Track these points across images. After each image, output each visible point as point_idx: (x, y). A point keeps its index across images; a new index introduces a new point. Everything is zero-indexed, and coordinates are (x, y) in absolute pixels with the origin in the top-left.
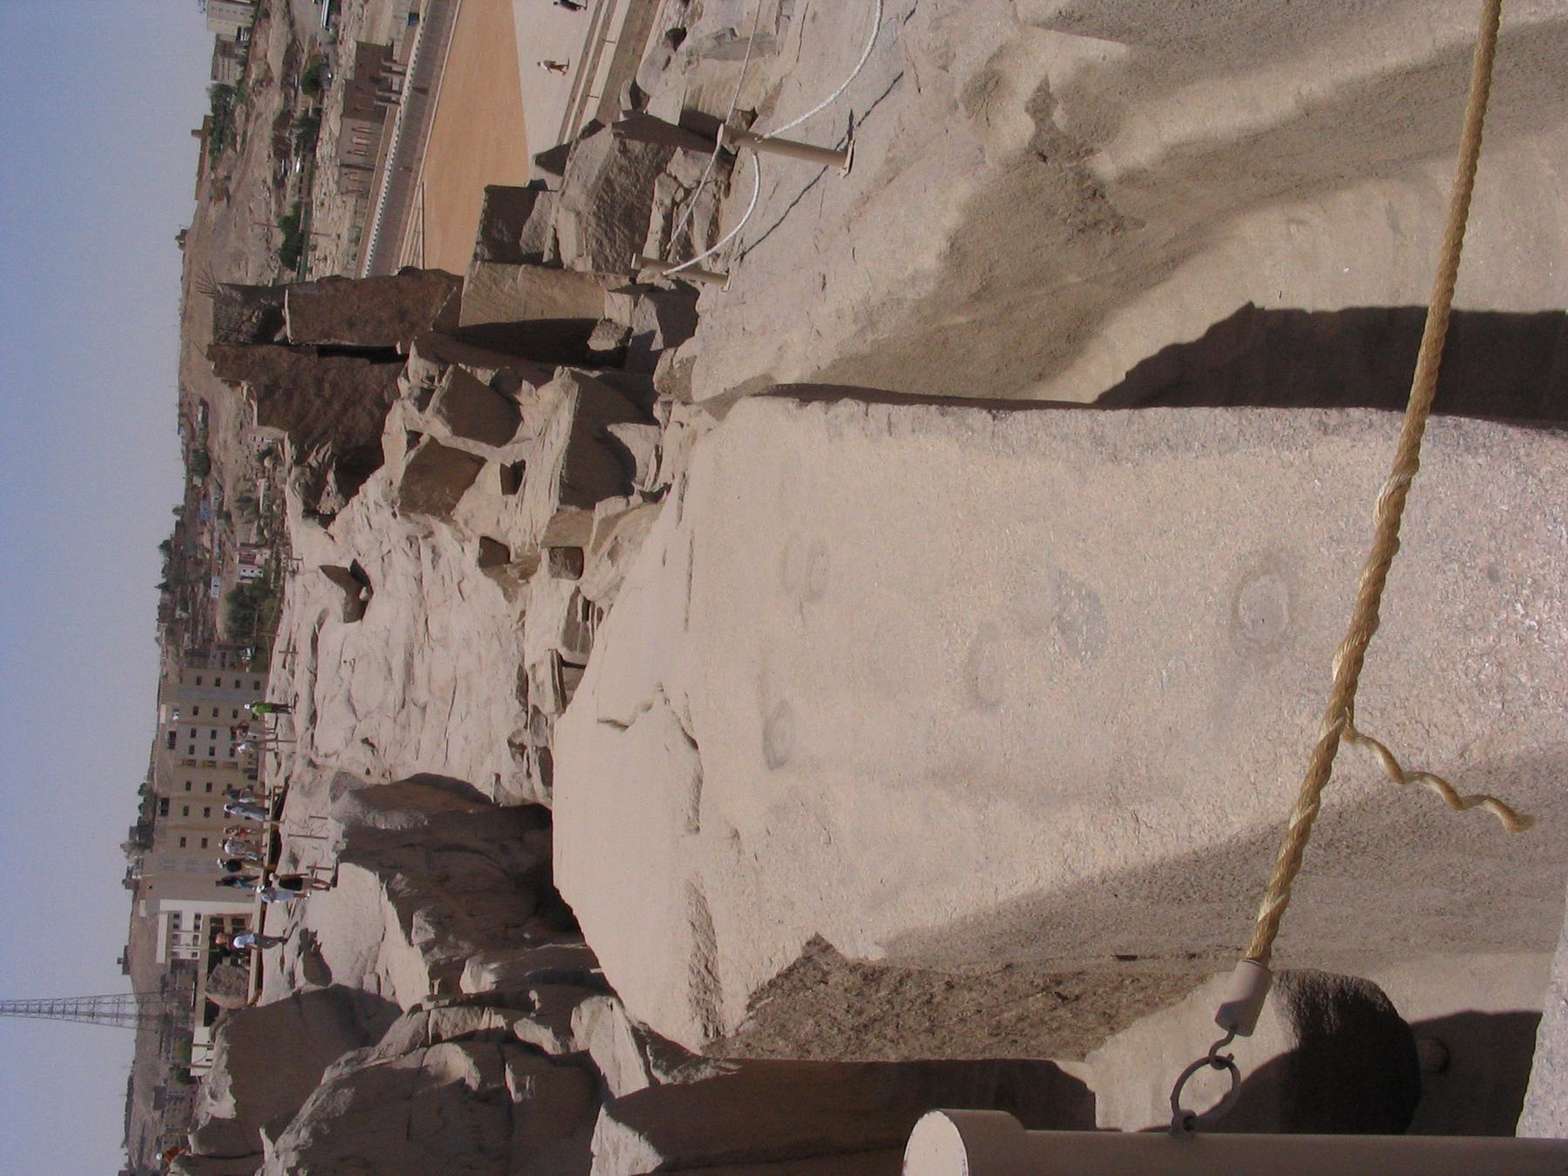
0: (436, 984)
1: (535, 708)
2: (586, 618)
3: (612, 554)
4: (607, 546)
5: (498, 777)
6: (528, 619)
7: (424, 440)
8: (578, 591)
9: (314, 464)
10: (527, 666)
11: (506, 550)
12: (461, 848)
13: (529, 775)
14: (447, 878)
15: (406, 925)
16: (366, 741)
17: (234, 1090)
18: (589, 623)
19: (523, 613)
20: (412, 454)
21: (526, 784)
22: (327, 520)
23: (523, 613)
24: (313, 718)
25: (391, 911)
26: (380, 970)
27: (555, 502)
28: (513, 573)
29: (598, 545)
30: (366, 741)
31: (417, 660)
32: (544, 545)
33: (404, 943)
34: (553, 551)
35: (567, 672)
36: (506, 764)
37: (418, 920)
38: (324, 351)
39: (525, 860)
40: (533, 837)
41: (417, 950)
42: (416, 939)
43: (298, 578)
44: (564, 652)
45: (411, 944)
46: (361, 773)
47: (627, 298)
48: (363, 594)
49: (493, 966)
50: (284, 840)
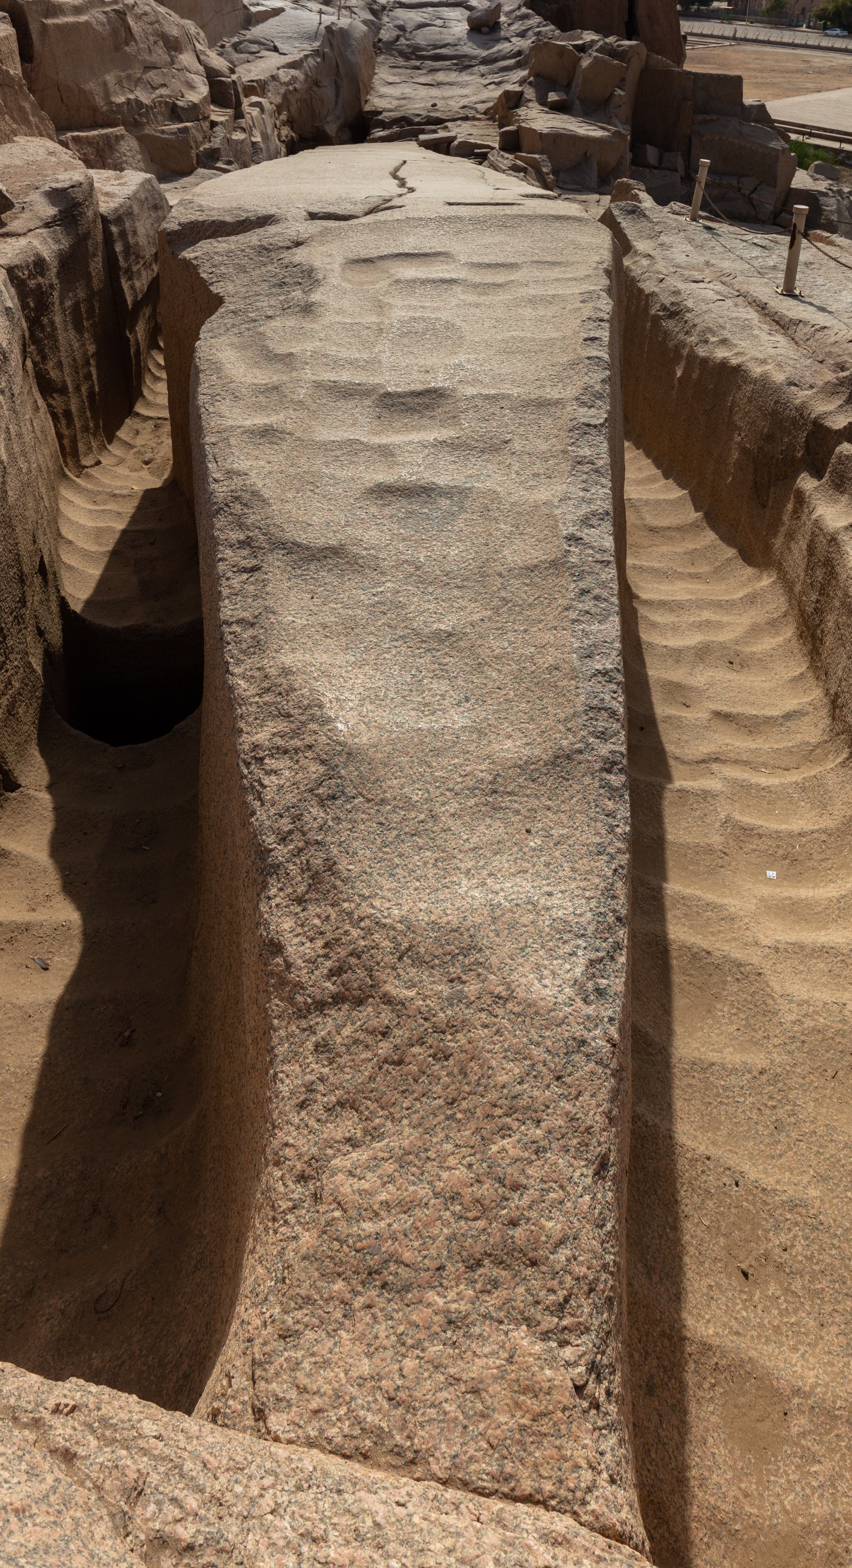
3: (515, 169)
4: (519, 162)
8: (493, 148)
11: (517, 106)
12: (337, 95)
14: (319, 86)
27: (546, 131)
29: (521, 159)
31: (448, 63)
32: (520, 127)
34: (516, 133)
35: (443, 147)
37: (293, 72)
39: (331, 129)
44: (456, 143)
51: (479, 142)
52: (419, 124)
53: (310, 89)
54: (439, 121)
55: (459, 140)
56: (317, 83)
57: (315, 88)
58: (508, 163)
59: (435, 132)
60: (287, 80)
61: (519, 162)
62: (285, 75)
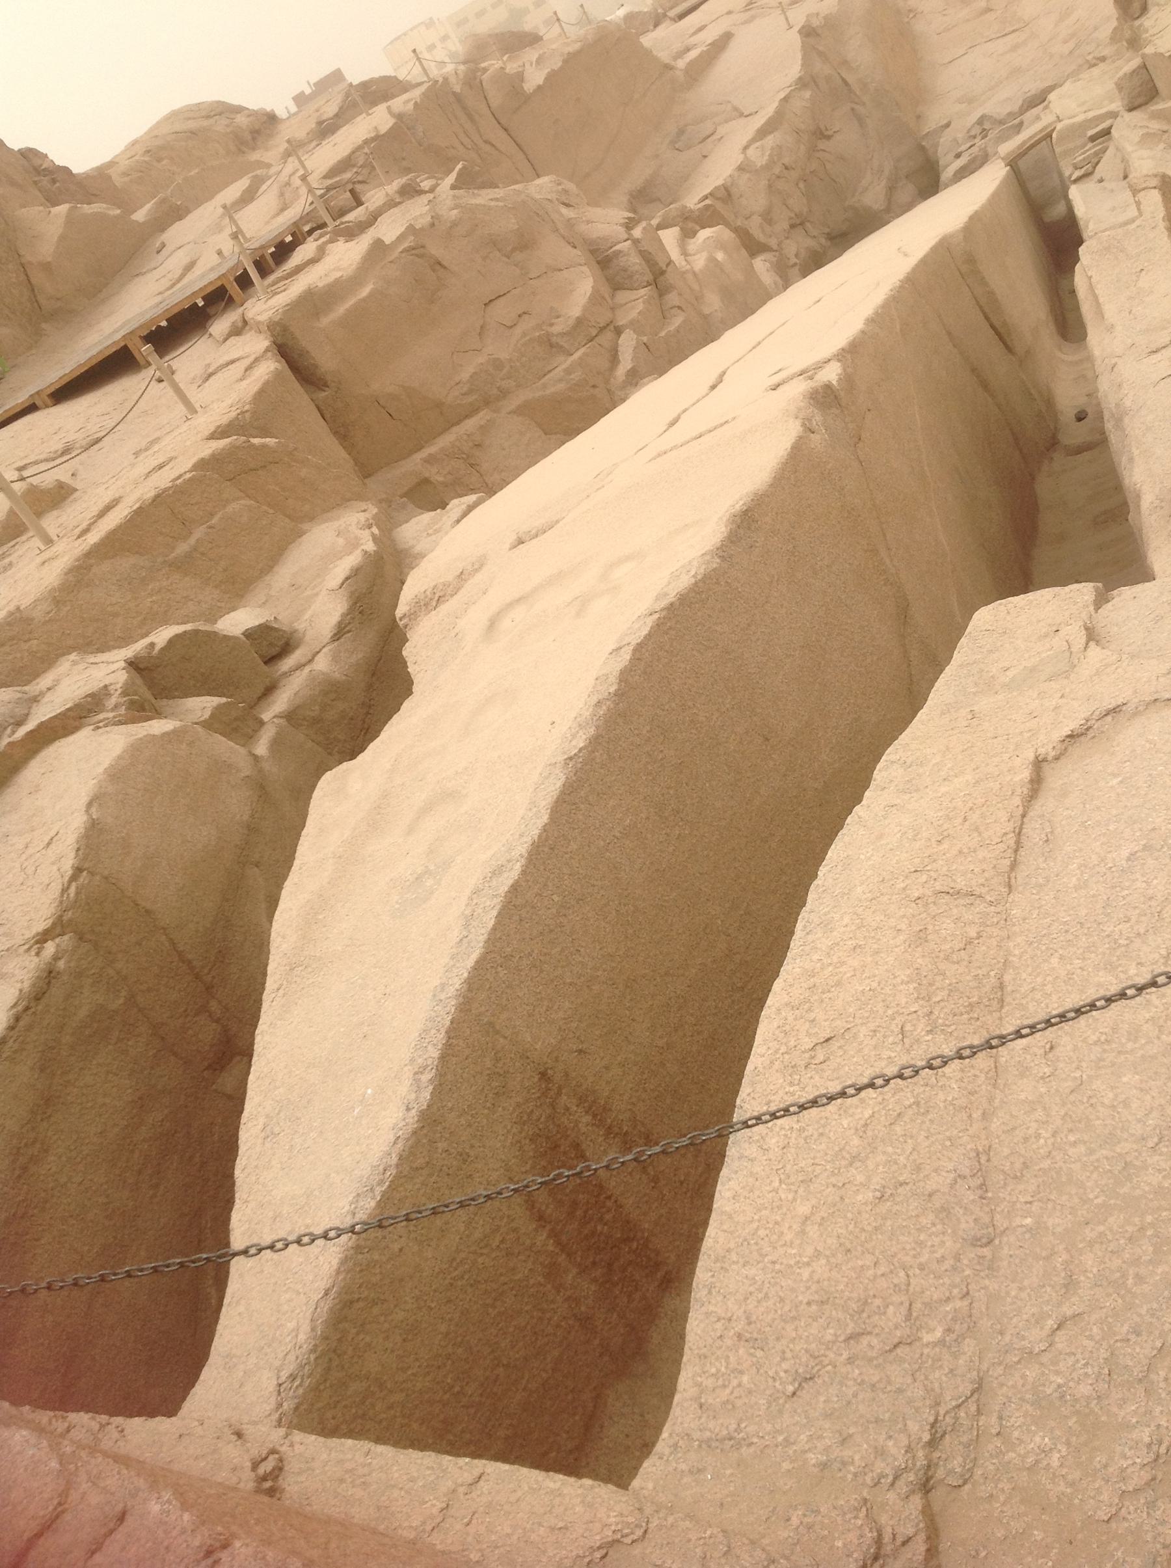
0: (708, 202)
1: (1021, 123)
2: (1093, 139)
5: (948, 125)
8: (1114, 115)
10: (1052, 97)
13: (958, 156)
15: (762, 133)
17: (551, 77)
18: (1090, 145)
19: (1103, 59)
21: (951, 156)
23: (1103, 59)
25: (770, 111)
26: (721, 131)
28: (1128, 34)
32: (1144, 56)
33: (744, 143)
34: (1144, 66)
36: (958, 130)
37: (770, 141)
40: (906, 191)
41: (741, 158)
42: (751, 152)
44: (1054, 135)
45: (746, 148)
49: (720, 256)
51: (1091, 115)
52: (1012, 115)
53: (813, 149)
54: (1039, 99)
55: (1059, 126)
56: (821, 134)
57: (822, 144)
58: (1136, 135)
59: (1038, 118)
60: (764, 160)
61: (1155, 126)
62: (758, 156)
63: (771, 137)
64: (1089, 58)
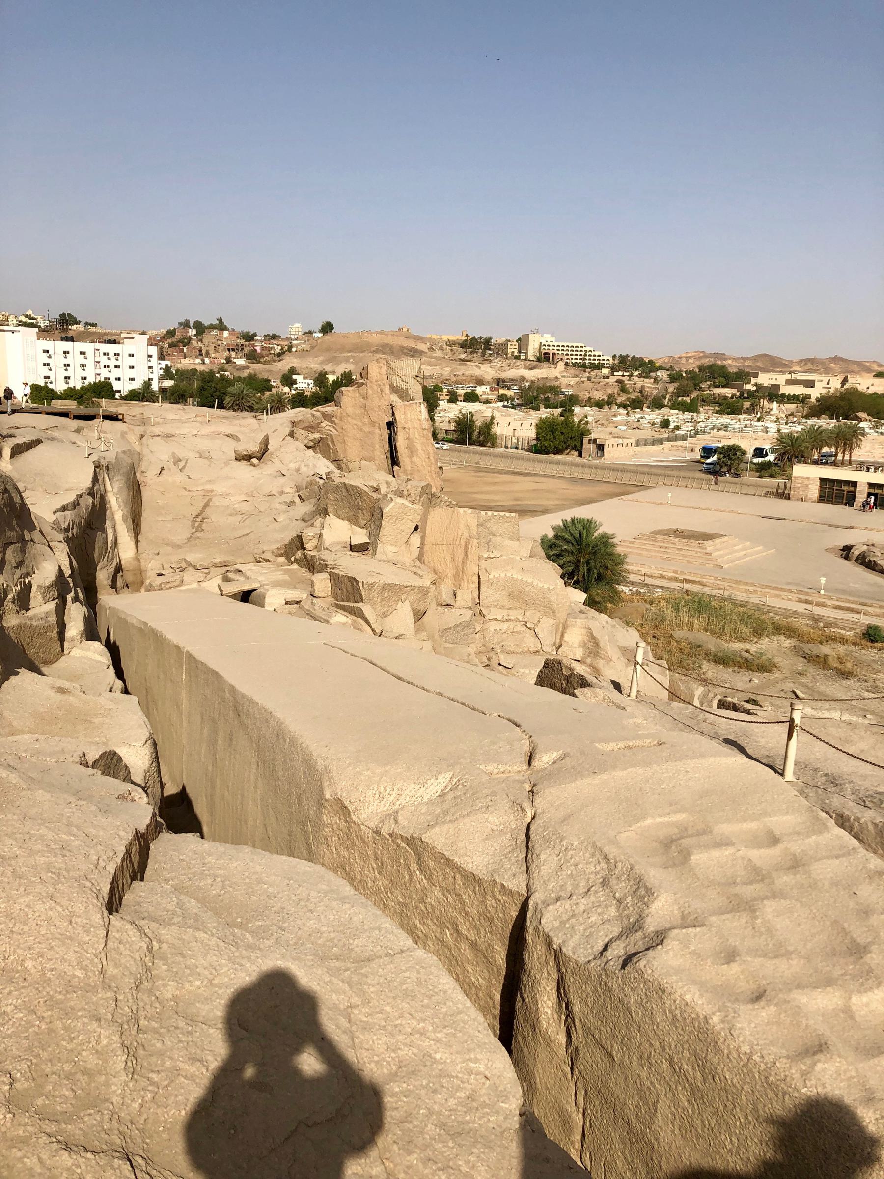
6: (264, 564)
7: (375, 495)
9: (323, 425)
15: (64, 509)
16: (162, 469)
20: (366, 489)
22: (291, 434)
23: (268, 561)
24: (168, 436)
25: (71, 498)
30: (162, 469)
38: (390, 425)
43: (254, 421)
46: (143, 469)
47: (470, 603)
48: (255, 461)
50: (90, 422)
63: (67, 512)
64: (257, 556)
